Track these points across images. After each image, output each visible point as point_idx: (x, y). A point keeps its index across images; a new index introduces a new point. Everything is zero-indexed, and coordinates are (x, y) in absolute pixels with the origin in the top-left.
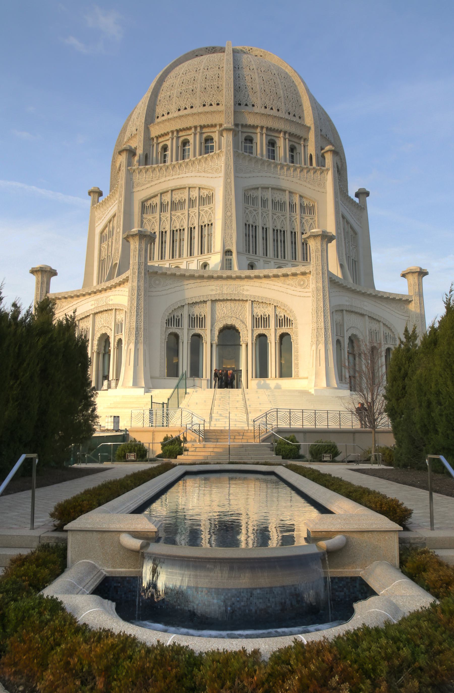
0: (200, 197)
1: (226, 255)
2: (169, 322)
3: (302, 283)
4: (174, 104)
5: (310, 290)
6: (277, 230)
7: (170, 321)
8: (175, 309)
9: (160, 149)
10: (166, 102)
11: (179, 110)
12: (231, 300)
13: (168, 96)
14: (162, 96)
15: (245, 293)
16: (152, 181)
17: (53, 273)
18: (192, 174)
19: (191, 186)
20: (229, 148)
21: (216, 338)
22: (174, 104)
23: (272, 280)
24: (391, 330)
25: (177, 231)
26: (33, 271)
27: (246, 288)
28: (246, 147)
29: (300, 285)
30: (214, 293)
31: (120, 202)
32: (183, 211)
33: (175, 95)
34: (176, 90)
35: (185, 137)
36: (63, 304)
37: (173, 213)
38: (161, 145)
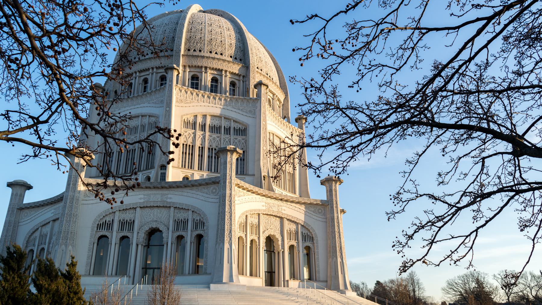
0: (149, 123)
1: (161, 169)
2: (100, 226)
3: (214, 191)
5: (218, 197)
6: (212, 149)
8: (106, 215)
12: (157, 206)
15: (169, 200)
17: (30, 187)
18: (146, 105)
19: (143, 114)
20: (170, 83)
21: (141, 240)
23: (191, 190)
24: (309, 230)
26: (10, 185)
27: (169, 196)
28: (192, 84)
29: (213, 193)
30: (142, 201)
32: (136, 135)
35: (145, 77)
36: (32, 213)
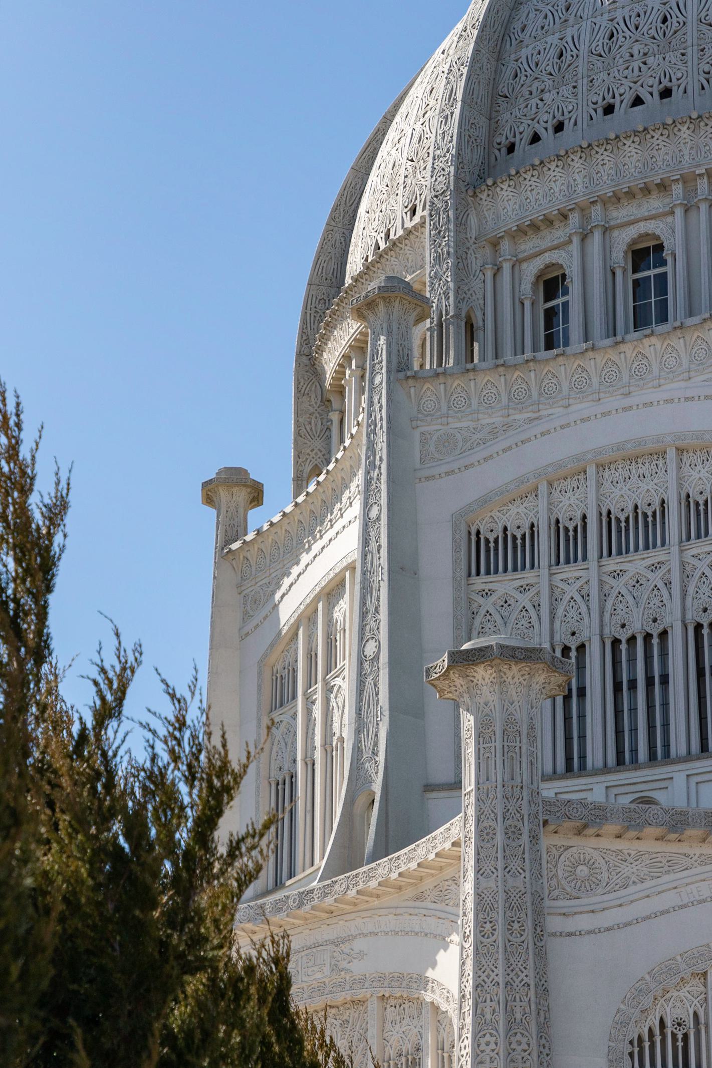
4: (583, 85)
7: (647, 1045)
9: (526, 286)
10: (546, 78)
11: (609, 110)
13: (553, 52)
14: (524, 52)
16: (507, 427)
22: (583, 85)
25: (632, 640)
31: (367, 524)
32: (656, 555)
33: (584, 47)
34: (586, 26)
37: (612, 564)
38: (531, 269)
